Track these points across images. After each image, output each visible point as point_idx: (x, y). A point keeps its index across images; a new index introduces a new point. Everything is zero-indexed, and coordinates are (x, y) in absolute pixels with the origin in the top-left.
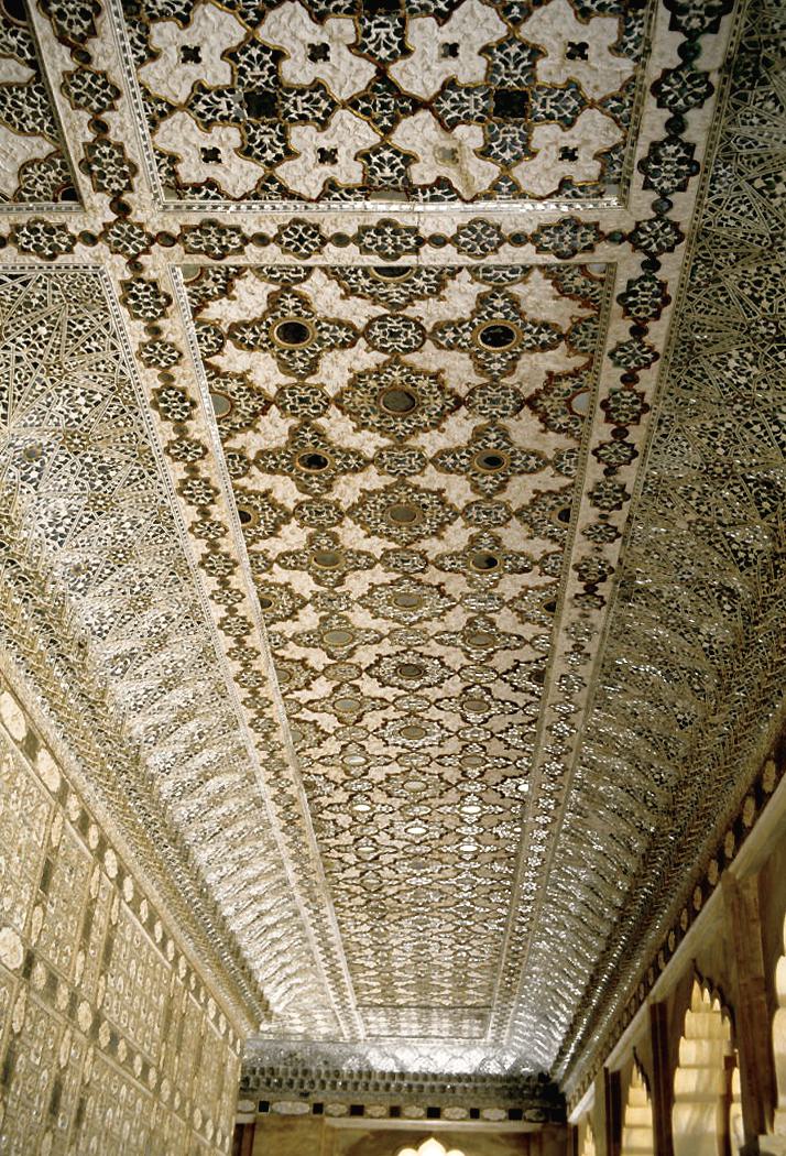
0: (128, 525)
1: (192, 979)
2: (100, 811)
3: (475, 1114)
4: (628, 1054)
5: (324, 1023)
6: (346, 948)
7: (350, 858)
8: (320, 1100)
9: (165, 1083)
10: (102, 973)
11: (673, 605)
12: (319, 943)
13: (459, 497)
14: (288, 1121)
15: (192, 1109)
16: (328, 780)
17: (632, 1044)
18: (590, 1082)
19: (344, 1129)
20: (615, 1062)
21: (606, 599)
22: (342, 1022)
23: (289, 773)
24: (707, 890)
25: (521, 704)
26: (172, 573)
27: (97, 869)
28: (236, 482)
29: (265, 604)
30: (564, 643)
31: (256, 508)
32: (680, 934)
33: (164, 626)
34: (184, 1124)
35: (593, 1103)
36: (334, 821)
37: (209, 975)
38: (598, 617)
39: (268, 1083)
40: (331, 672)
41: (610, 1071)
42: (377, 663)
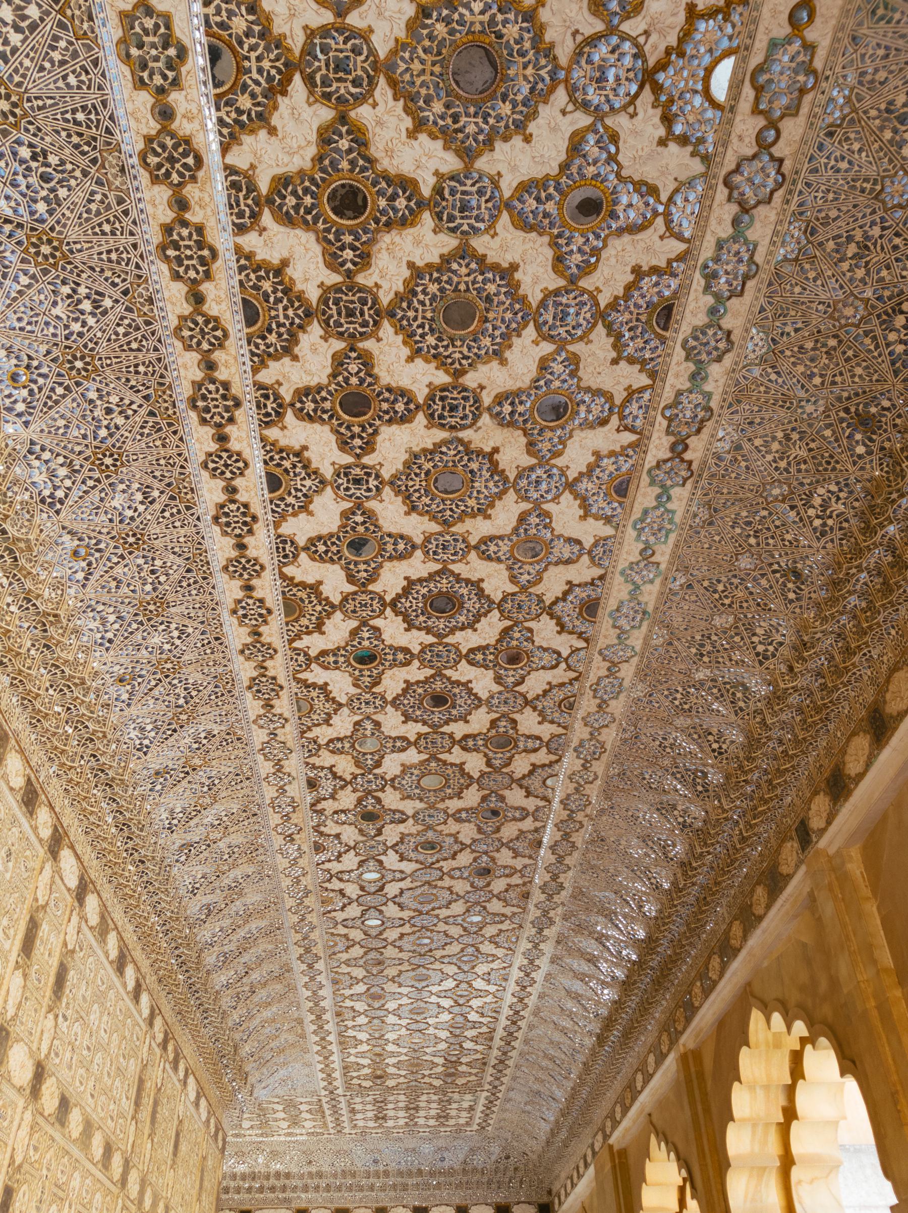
0: (86, 306)
1: (170, 1048)
2: (54, 789)
5: (308, 1116)
6: (338, 1014)
7: (352, 890)
9: (134, 1177)
10: (50, 1010)
11: (783, 464)
12: (310, 1010)
13: (536, 280)
17: (647, 1110)
18: (586, 1166)
21: (695, 466)
22: (328, 1112)
24: (775, 882)
25: (565, 653)
26: (152, 414)
27: (48, 866)
28: (240, 240)
29: (274, 483)
30: (629, 550)
31: (266, 296)
32: (727, 950)
33: (141, 508)
38: (680, 498)
40: (350, 607)
41: (616, 1148)
42: (406, 591)
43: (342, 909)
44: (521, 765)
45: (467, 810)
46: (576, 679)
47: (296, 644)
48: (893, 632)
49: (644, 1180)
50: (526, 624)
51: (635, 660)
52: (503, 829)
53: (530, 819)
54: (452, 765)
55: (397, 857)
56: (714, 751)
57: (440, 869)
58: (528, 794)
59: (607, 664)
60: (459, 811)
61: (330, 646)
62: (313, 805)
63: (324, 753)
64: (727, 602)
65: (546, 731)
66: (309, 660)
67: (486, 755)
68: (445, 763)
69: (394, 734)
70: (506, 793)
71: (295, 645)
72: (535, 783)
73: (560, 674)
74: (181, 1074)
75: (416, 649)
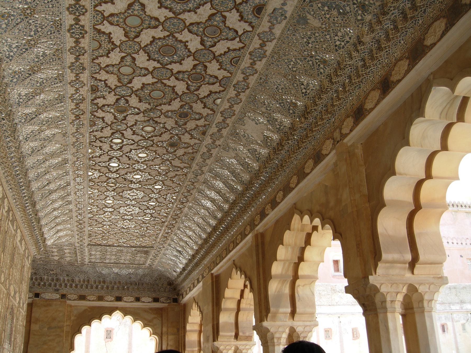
3: (138, 299)
4: (230, 263)
8: (65, 293)
14: (49, 302)
15: (10, 285)
16: (106, 85)
17: (233, 259)
18: (198, 282)
19: (76, 306)
20: (217, 271)
23: (85, 77)
24: (318, 158)
32: (287, 190)
34: (6, 292)
35: (201, 289)
36: (103, 118)
37: (18, 215)
39: (39, 284)
43: (99, 157)
44: (204, 91)
45: (172, 111)
46: (243, 48)
47: (98, 8)
48: (402, 42)
49: (227, 286)
50: (224, 13)
51: (274, 42)
52: (188, 123)
53: (203, 120)
54: (169, 86)
55: (132, 132)
56: (303, 93)
57: (152, 141)
58: (205, 106)
59: (261, 42)
60: (168, 111)
61: (116, 12)
62: (93, 100)
63: (103, 72)
64: (328, 16)
65: (221, 74)
66: (104, 18)
67: (187, 83)
68: (165, 85)
69: (141, 66)
70: (194, 105)
71: (97, 8)
72: (209, 101)
73: (236, 44)
74: (15, 227)
75: (162, 19)
